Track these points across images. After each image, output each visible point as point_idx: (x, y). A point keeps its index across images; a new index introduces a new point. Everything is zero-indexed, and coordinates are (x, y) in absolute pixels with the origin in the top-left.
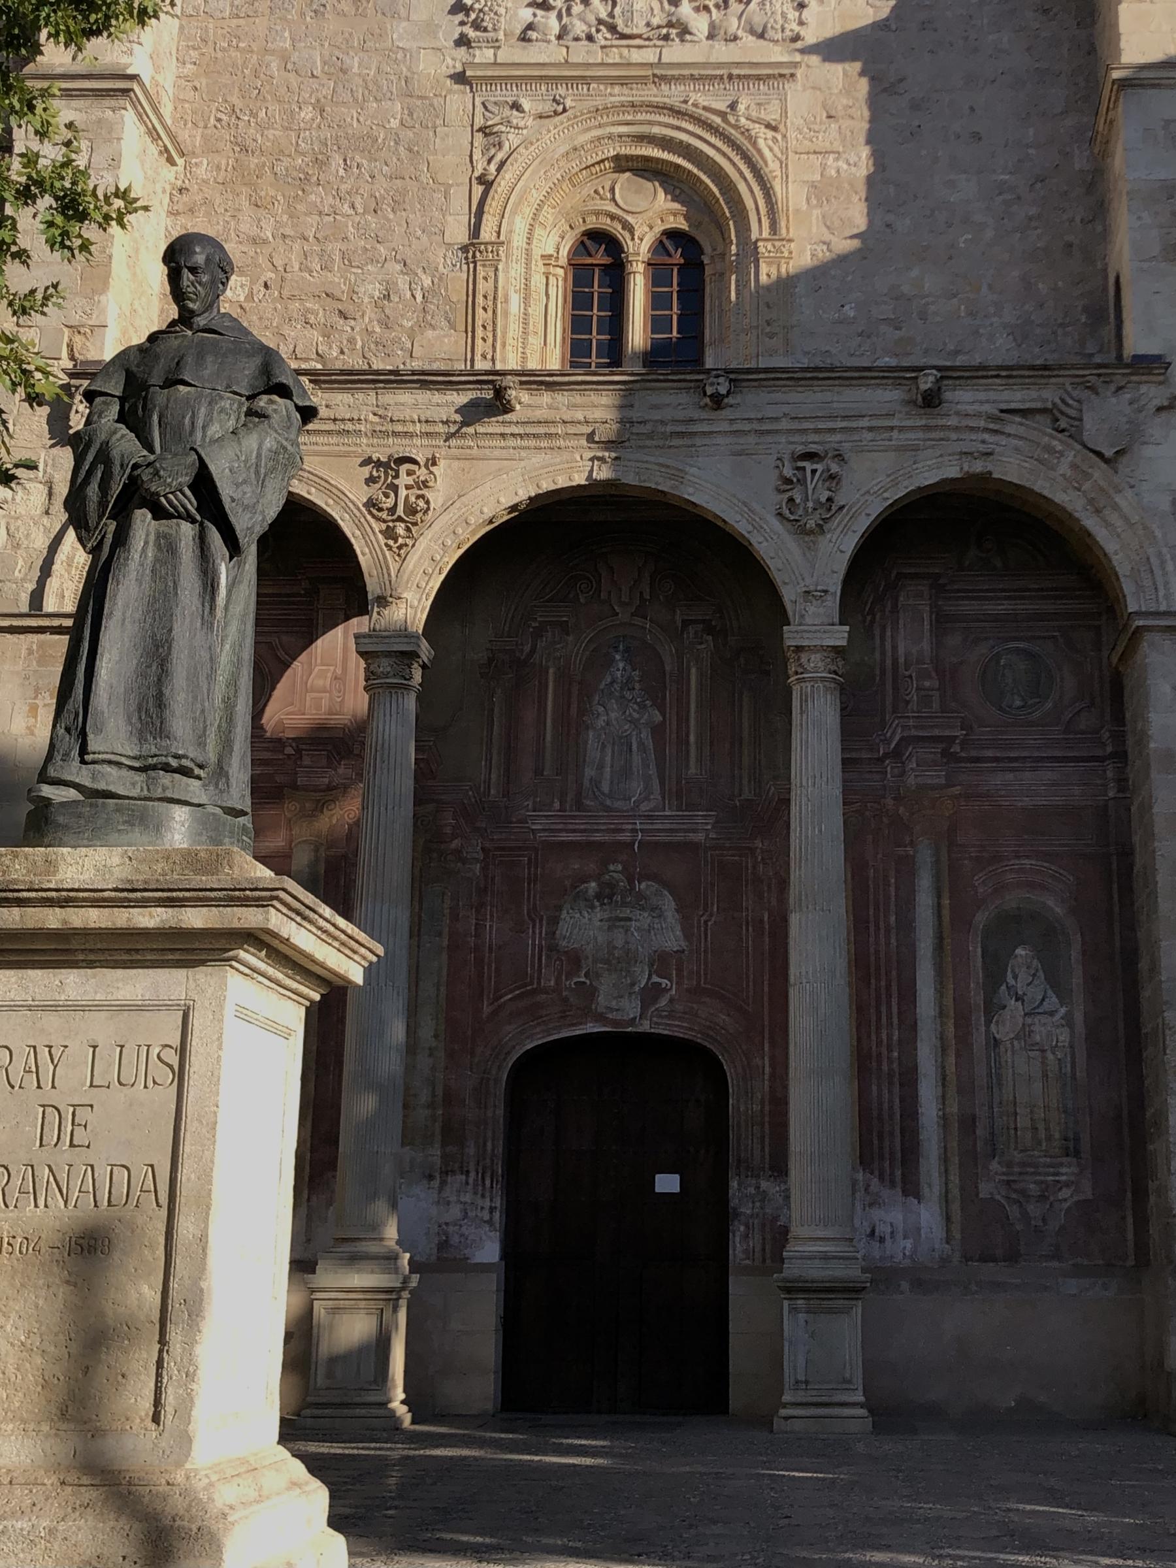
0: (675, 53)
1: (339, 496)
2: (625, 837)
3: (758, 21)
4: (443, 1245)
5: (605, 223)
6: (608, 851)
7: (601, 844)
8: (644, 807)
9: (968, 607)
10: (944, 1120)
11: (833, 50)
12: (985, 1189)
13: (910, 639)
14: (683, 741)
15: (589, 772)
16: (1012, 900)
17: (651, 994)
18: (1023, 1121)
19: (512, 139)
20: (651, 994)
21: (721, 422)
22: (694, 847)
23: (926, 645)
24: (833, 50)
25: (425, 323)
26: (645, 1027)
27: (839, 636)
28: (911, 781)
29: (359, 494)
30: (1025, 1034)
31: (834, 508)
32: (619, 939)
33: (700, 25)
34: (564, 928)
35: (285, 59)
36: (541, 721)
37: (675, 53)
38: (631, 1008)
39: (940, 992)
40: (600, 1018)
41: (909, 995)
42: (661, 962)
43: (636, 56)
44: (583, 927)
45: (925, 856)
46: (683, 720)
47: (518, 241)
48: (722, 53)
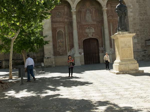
2: (90, 24)
6: (88, 25)
7: (88, 25)
8: (91, 22)
9: (113, 5)
14: (93, 17)
15: (87, 19)
17: (92, 35)
20: (92, 35)
22: (94, 24)
23: (110, 9)
26: (92, 38)
27: (107, 9)
28: (110, 19)
32: (90, 31)
34: (86, 31)
36: (83, 16)
38: (91, 36)
40: (89, 37)
42: (93, 33)
44: (87, 31)
45: (111, 24)
46: (93, 15)
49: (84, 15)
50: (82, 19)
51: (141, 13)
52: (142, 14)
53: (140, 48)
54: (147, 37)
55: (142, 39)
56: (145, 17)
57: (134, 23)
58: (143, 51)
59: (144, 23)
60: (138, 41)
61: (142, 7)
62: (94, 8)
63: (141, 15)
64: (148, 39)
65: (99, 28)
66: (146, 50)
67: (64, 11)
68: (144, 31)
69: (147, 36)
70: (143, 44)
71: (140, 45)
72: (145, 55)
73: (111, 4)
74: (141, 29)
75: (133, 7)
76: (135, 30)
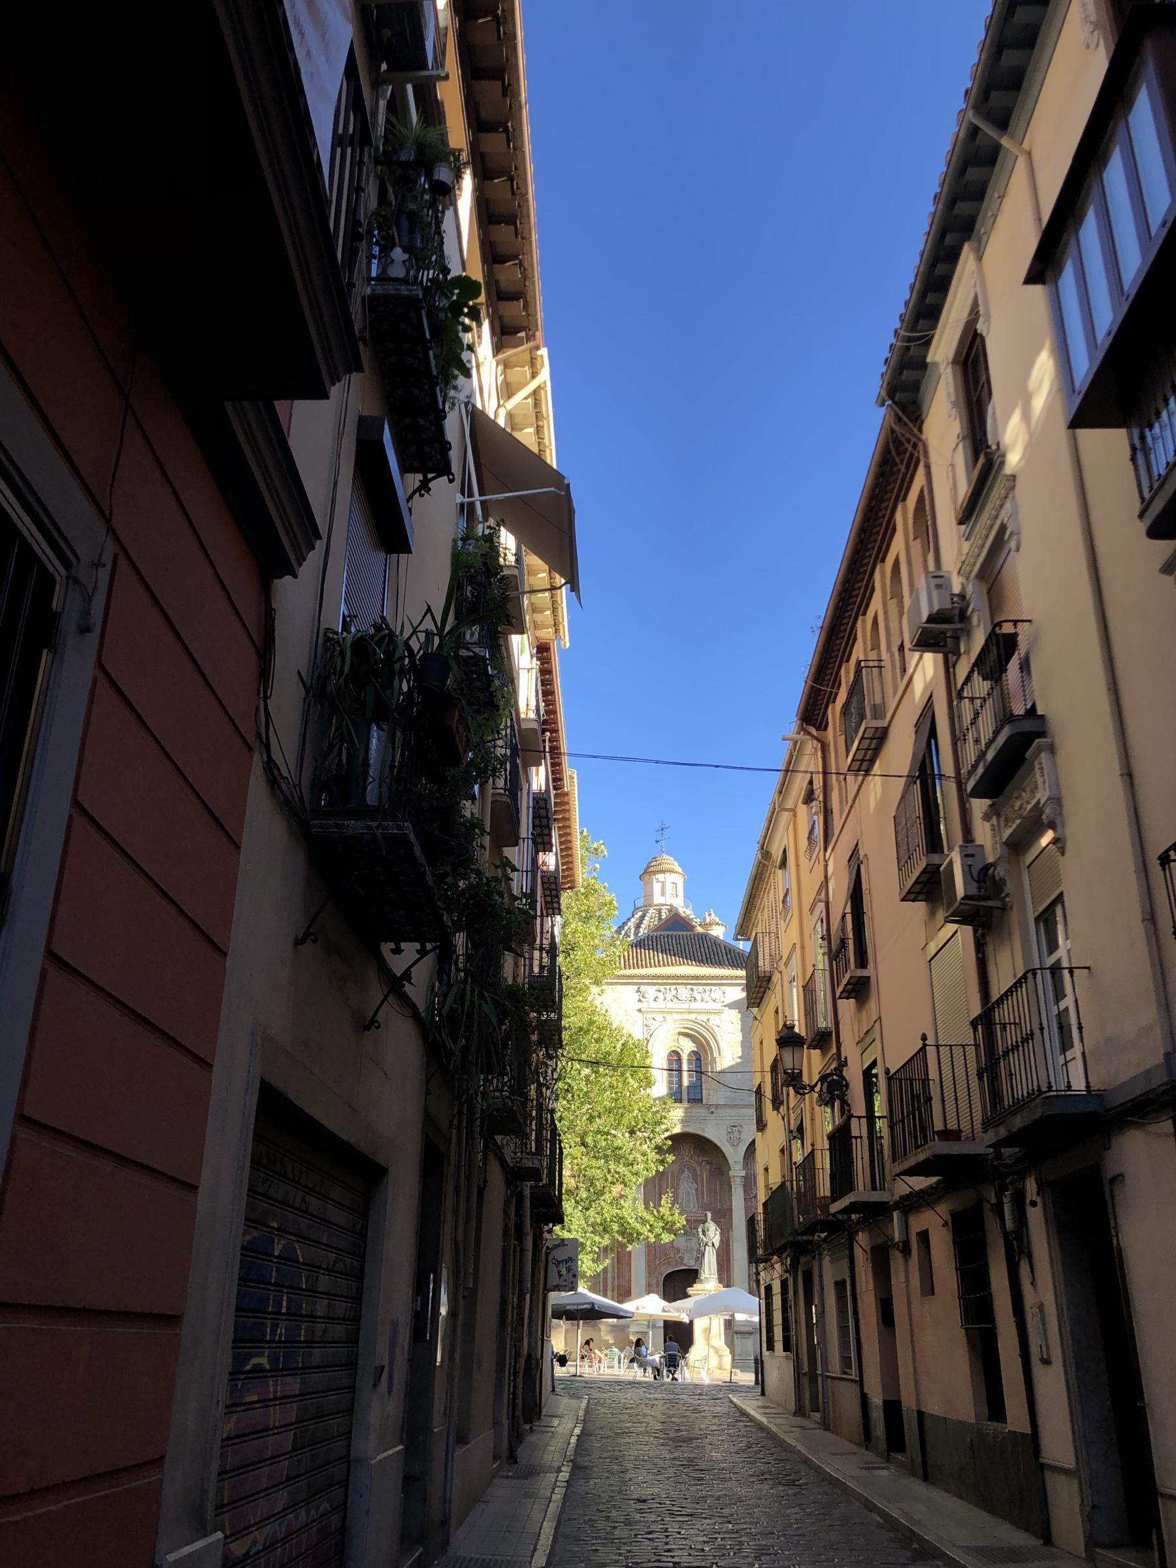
0: (694, 1005)
11: (731, 1006)
19: (653, 1028)
21: (713, 1117)
24: (731, 1006)
33: (699, 997)
37: (694, 1005)
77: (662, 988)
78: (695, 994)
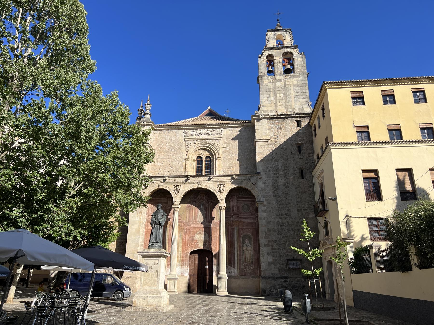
0: (208, 137)
1: (171, 189)
3: (217, 133)
4: (182, 274)
5: (200, 155)
9: (240, 199)
10: (238, 259)
12: (242, 267)
13: (234, 203)
16: (245, 234)
18: (246, 259)
19: (189, 146)
25: (180, 168)
28: (234, 220)
29: (173, 189)
30: (247, 249)
31: (158, 295)
33: (210, 133)
35: (165, 138)
39: (237, 244)
41: (234, 245)
43: (204, 137)
45: (236, 228)
47: (191, 158)
48: (213, 137)
49: (195, 213)
50: (191, 218)
51: (280, 214)
52: (282, 215)
53: (277, 272)
54: (290, 254)
55: (281, 256)
56: (286, 221)
57: (268, 229)
58: (281, 278)
59: (285, 230)
60: (273, 260)
61: (283, 204)
62: (211, 202)
63: (281, 216)
64: (291, 258)
65: (216, 234)
66: (286, 278)
67: (167, 205)
68: (285, 244)
69: (289, 253)
70: (283, 266)
71: (277, 266)
72: (286, 285)
73: (237, 197)
74: (280, 240)
75: (268, 203)
76: (269, 241)
77: (195, 131)
78: (209, 132)
